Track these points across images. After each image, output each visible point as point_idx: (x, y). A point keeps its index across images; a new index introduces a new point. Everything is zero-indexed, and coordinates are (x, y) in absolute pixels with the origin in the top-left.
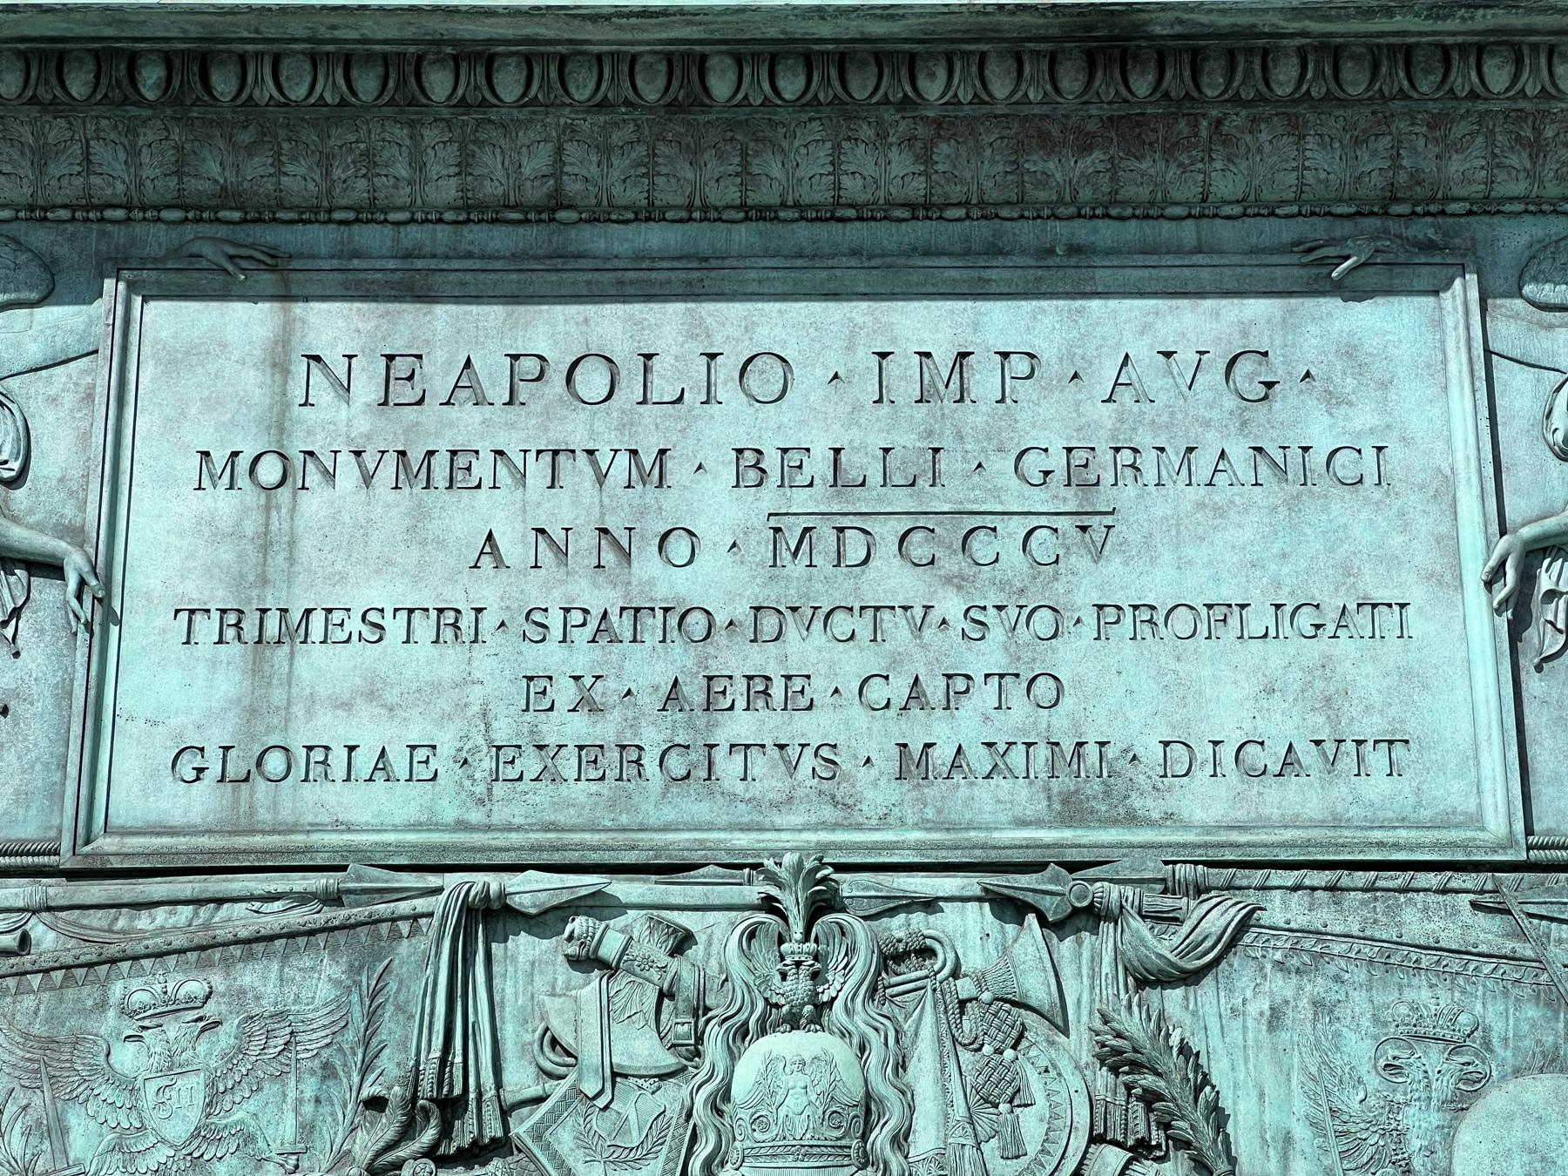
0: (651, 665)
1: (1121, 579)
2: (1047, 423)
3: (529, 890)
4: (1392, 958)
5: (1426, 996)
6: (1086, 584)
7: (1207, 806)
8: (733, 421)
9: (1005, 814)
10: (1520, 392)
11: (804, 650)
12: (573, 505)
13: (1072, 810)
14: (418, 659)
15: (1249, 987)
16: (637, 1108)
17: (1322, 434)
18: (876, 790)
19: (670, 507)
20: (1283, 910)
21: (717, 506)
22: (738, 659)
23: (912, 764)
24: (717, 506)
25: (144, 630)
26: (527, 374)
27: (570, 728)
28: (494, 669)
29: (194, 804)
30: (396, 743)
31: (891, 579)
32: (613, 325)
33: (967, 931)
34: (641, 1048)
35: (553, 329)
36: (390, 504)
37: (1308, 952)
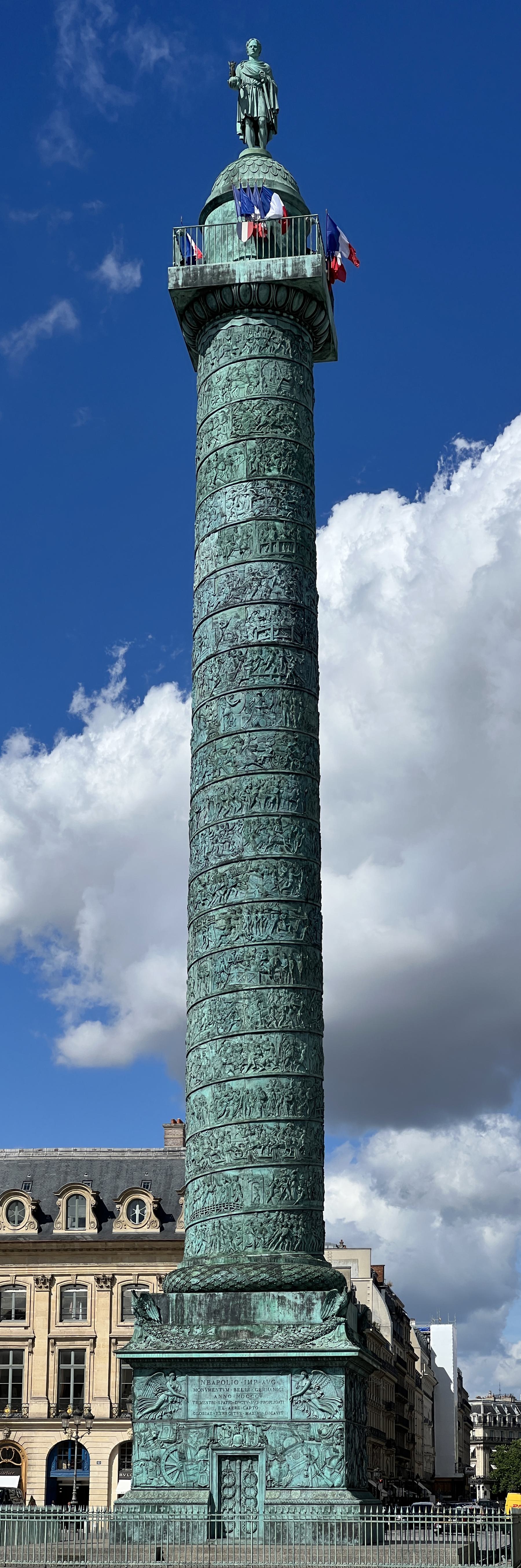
0: (228, 1406)
1: (263, 1399)
2: (258, 1386)
3: (219, 1424)
4: (280, 1429)
6: (260, 1399)
7: (268, 1417)
8: (234, 1386)
9: (254, 1418)
10: (294, 1383)
11: (239, 1404)
12: (221, 1393)
13: (258, 1417)
14: (211, 1405)
15: (270, 1431)
16: (227, 1440)
18: (244, 1416)
19: (229, 1393)
21: (233, 1393)
22: (234, 1405)
23: (247, 1414)
24: (233, 1393)
25: (190, 1403)
26: (218, 1382)
28: (216, 1406)
29: (195, 1417)
30: (209, 1412)
31: (246, 1399)
32: (224, 1378)
33: (250, 1426)
34: (227, 1436)
35: (220, 1378)
36: (208, 1393)
37: (275, 1429)
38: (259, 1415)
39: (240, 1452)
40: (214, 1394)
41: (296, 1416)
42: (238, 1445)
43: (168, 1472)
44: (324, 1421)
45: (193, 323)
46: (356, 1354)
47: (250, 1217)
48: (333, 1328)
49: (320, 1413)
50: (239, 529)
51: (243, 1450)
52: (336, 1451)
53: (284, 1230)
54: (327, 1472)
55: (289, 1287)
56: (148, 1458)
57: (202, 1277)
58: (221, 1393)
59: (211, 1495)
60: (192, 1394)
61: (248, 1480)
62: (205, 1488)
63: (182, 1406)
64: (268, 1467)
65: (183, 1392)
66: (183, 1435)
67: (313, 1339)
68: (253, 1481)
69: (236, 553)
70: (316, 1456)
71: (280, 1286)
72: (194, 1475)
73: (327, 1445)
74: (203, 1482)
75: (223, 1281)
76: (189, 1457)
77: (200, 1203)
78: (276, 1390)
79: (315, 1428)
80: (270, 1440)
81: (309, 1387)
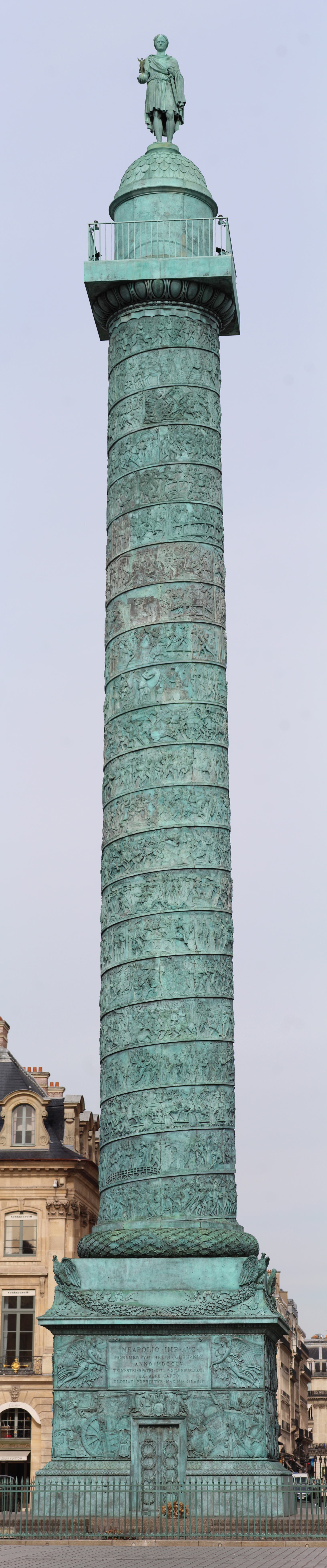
0: (148, 1374)
2: (178, 1354)
4: (201, 1398)
5: (203, 1400)
7: (189, 1385)
8: (154, 1354)
9: (174, 1386)
10: (214, 1351)
11: (160, 1372)
14: (131, 1373)
16: (148, 1409)
17: (199, 1354)
18: (165, 1384)
20: (194, 1394)
22: (155, 1373)
23: (167, 1382)
24: (153, 1360)
27: (143, 1379)
28: (137, 1374)
29: (116, 1385)
33: (171, 1396)
34: (148, 1404)
36: (129, 1361)
38: (180, 1382)
39: (160, 1422)
40: (136, 1361)
41: (216, 1384)
42: (158, 1415)
43: (89, 1442)
44: (243, 1389)
45: (105, 309)
46: (276, 1321)
47: (168, 1181)
48: (253, 1295)
49: (240, 1381)
50: (152, 511)
51: (163, 1419)
52: (256, 1420)
54: (247, 1442)
55: (206, 1252)
56: (69, 1428)
57: (121, 1242)
58: (142, 1361)
59: (132, 1467)
60: (112, 1362)
61: (168, 1450)
62: (127, 1459)
63: (103, 1374)
64: (189, 1436)
65: (103, 1360)
66: (103, 1404)
67: (233, 1305)
68: (173, 1451)
69: (149, 534)
70: (237, 1425)
71: (198, 1252)
72: (114, 1445)
73: (248, 1414)
74: (124, 1453)
75: (142, 1245)
76: (110, 1427)
77: (117, 1168)
78: (197, 1358)
79: (235, 1396)
80: (190, 1409)
81: (229, 1355)
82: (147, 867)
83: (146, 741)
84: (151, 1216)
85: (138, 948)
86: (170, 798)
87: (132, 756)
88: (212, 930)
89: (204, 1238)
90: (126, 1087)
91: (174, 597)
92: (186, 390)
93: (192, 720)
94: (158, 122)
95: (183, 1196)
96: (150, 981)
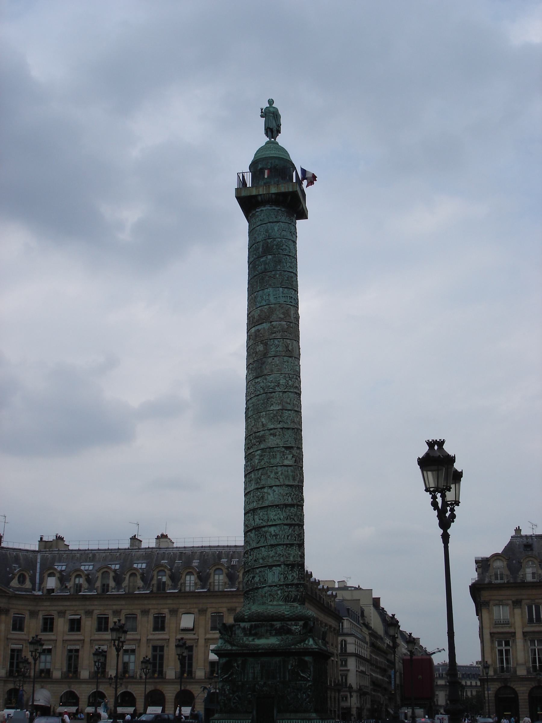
53: (286, 594)
82: (262, 446)
83: (262, 391)
84: (264, 603)
85: (258, 483)
86: (272, 415)
87: (256, 398)
88: (291, 474)
89: (286, 613)
90: (254, 545)
91: (274, 328)
92: (279, 240)
93: (282, 382)
94: (269, 133)
95: (278, 594)
96: (263, 497)
